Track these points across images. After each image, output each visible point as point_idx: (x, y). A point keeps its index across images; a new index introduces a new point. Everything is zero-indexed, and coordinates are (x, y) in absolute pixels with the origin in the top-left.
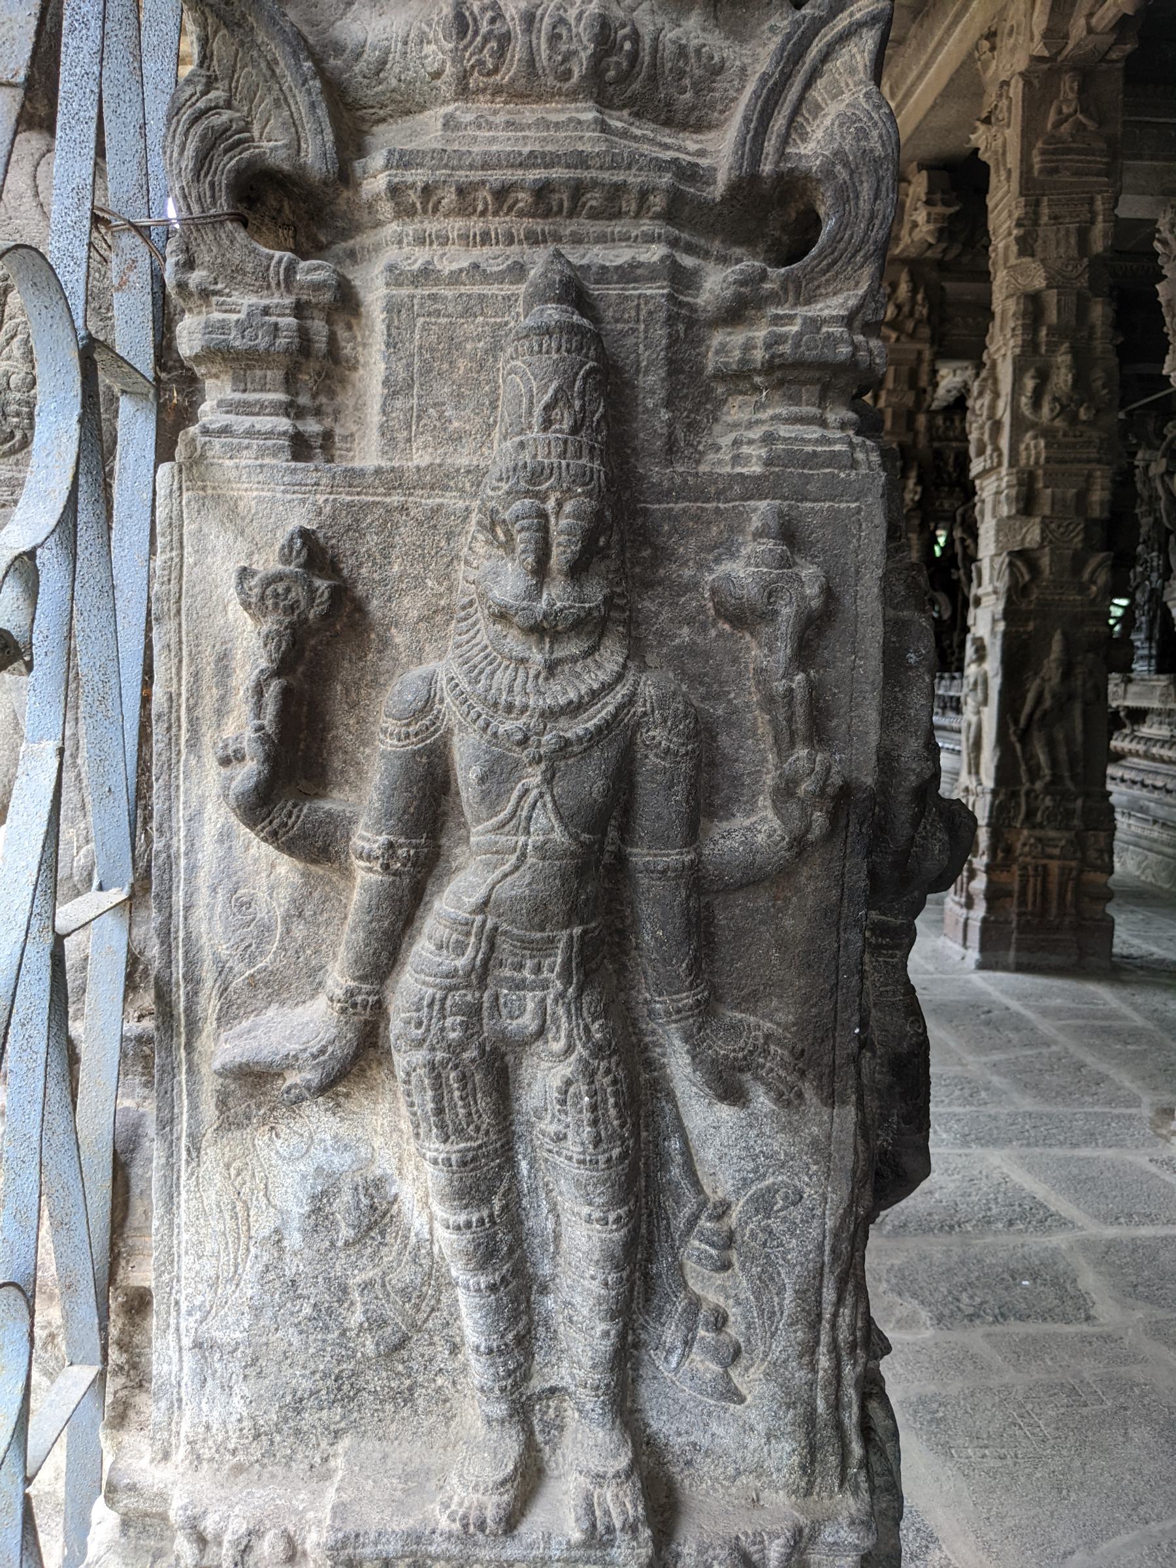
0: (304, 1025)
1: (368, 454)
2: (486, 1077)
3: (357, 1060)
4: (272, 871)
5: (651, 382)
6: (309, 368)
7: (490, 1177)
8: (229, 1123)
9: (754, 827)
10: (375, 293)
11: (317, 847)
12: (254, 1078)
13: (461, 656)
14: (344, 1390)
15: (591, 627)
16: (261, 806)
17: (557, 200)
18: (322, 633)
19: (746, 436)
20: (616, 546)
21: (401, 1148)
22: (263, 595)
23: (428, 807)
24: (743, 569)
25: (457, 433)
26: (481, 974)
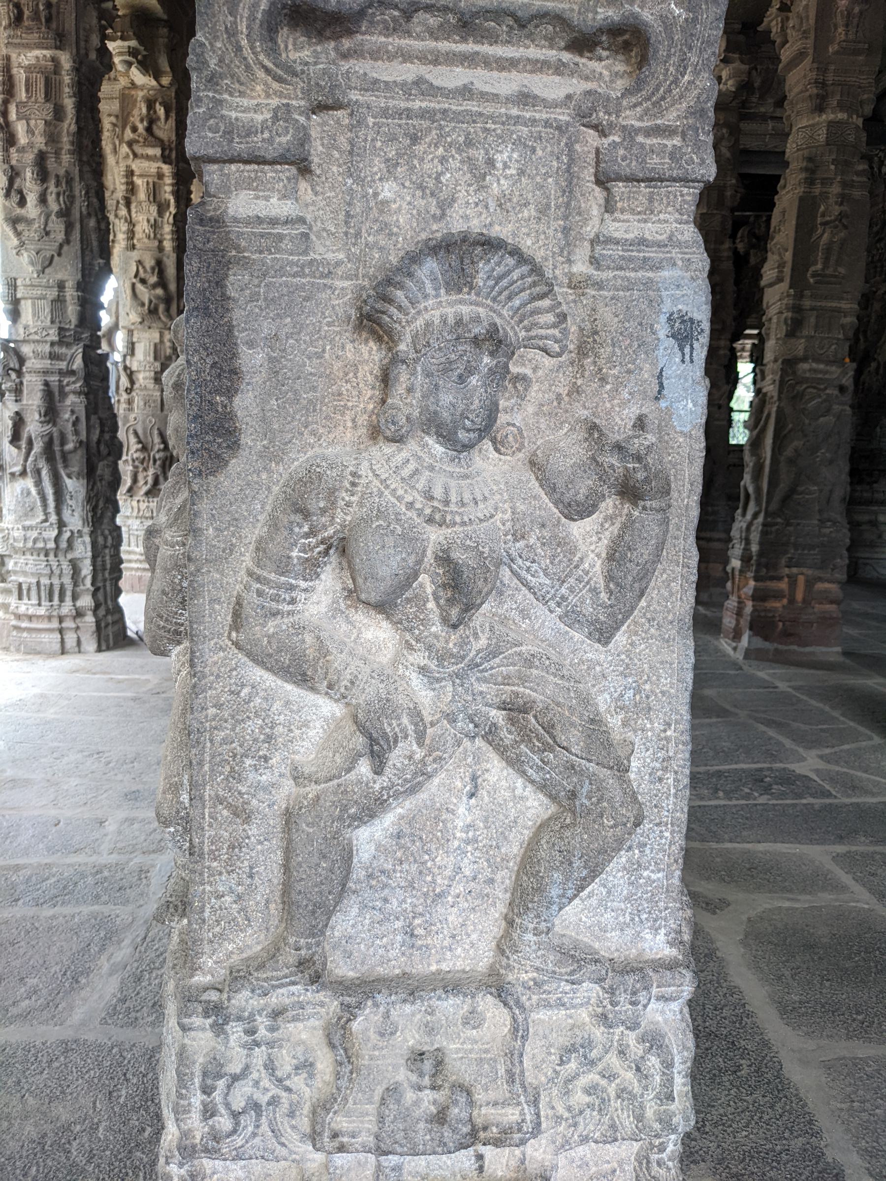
0: (17, 469)
1: (24, 402)
2: (38, 472)
3: (23, 473)
4: (15, 451)
5: (57, 394)
6: (18, 391)
7: (38, 483)
9: (70, 446)
12: (13, 475)
13: (34, 427)
14: (26, 515)
15: (48, 422)
16: (11, 442)
17: (46, 372)
18: (19, 422)
19: (71, 399)
20: (50, 413)
21: (29, 483)
22: (11, 418)
23: (30, 443)
24: (67, 416)
25: (33, 400)
26: (35, 460)
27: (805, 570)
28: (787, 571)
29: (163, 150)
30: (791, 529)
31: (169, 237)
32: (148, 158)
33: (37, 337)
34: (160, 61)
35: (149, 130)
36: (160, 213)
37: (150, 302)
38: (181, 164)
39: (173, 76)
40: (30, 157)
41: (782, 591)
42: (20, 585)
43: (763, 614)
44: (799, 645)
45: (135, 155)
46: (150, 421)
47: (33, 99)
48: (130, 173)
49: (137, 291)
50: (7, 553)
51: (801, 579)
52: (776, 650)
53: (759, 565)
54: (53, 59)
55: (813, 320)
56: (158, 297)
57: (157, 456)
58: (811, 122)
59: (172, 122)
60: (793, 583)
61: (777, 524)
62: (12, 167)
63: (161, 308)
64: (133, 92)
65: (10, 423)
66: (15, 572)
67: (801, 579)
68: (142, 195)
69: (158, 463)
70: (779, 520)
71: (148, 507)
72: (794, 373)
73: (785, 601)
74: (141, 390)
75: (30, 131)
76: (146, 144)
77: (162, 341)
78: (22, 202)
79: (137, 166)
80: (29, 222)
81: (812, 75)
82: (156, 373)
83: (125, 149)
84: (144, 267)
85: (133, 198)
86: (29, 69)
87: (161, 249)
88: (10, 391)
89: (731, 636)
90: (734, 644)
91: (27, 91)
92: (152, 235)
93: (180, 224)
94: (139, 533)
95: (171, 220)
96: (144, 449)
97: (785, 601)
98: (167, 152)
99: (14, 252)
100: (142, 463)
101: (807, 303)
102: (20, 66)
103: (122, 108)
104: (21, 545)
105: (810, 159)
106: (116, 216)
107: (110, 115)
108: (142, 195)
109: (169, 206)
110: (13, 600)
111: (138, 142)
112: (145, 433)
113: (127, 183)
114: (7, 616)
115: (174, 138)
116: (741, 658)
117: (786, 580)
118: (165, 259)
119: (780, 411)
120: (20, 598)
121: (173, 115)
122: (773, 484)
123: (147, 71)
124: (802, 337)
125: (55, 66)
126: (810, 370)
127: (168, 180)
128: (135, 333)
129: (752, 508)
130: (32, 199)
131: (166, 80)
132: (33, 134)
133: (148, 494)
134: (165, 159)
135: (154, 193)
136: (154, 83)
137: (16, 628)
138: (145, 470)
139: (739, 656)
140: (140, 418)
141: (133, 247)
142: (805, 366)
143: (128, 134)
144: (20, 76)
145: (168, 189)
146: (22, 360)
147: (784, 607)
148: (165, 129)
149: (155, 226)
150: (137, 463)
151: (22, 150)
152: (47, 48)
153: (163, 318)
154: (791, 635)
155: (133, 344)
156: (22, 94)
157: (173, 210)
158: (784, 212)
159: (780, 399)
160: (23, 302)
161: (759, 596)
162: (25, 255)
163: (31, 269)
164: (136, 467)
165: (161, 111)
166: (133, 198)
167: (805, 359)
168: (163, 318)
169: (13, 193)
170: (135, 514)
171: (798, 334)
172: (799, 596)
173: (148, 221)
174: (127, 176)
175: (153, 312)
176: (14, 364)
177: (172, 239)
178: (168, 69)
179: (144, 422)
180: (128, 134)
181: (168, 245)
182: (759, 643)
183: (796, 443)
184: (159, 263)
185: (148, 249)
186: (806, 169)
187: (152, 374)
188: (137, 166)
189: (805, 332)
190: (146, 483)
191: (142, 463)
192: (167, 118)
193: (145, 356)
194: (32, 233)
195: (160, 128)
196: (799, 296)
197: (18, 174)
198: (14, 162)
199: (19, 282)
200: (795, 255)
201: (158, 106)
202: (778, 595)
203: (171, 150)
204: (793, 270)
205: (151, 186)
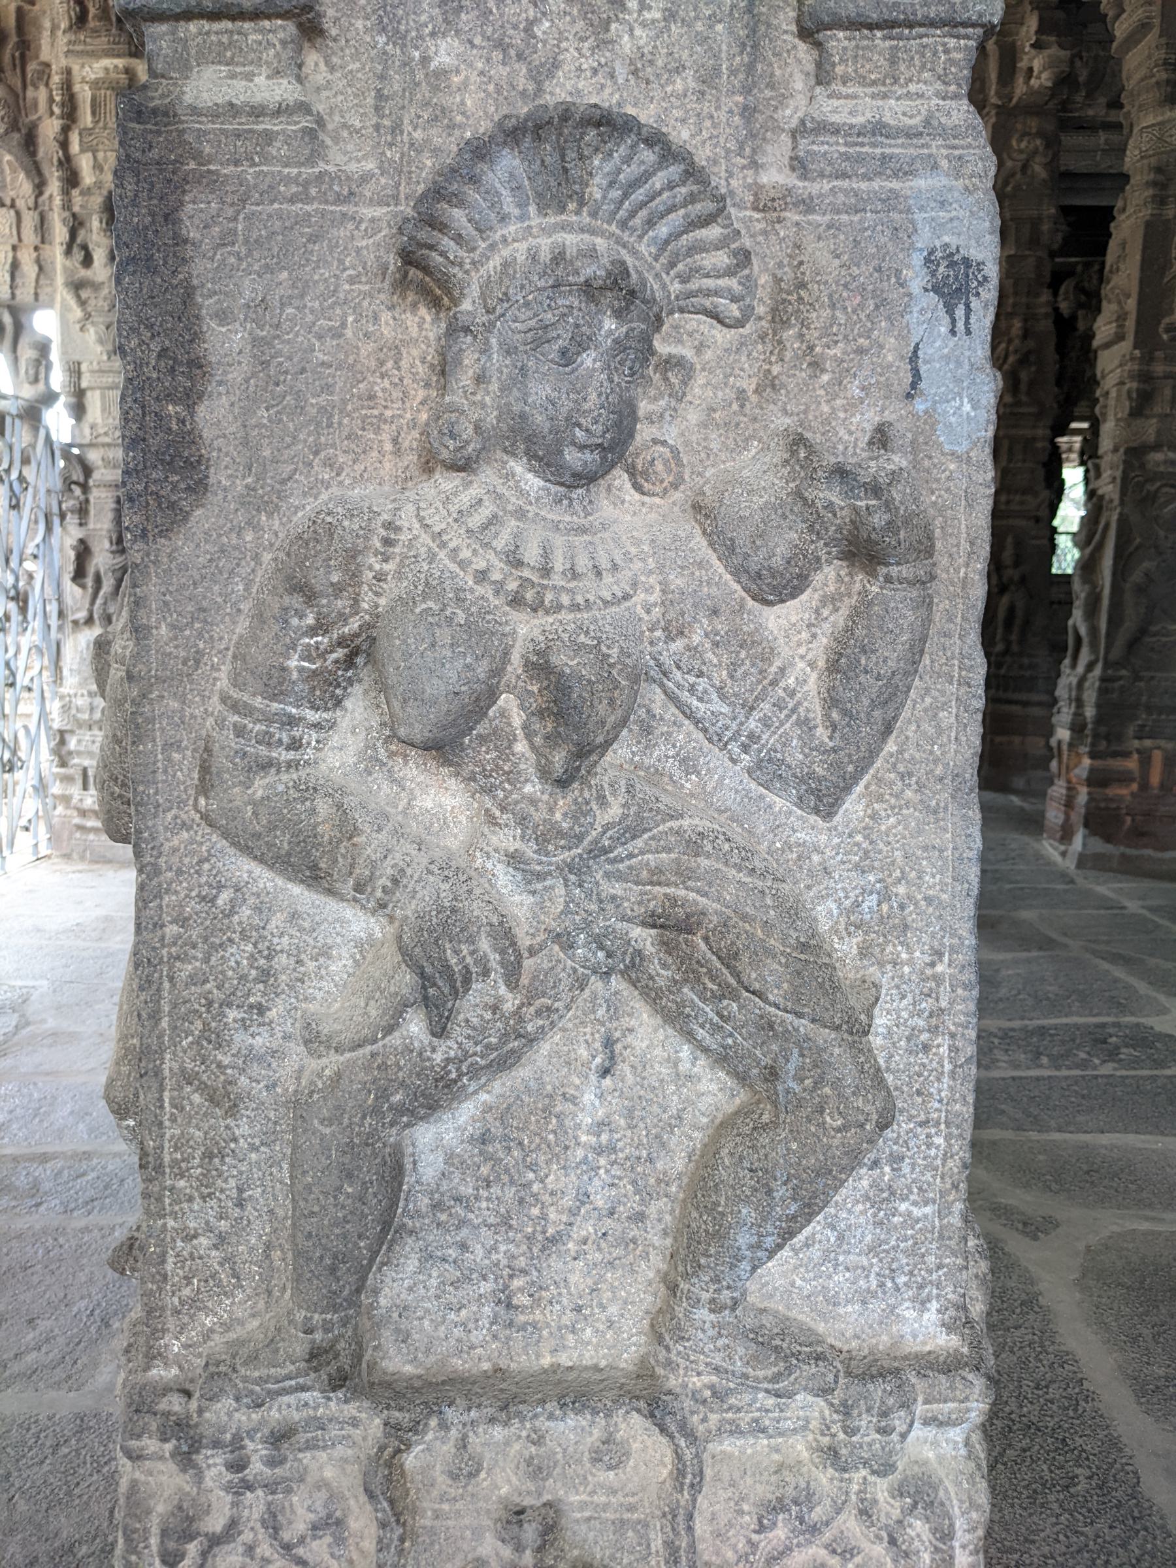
0: (82, 615)
1: (91, 526)
3: (89, 621)
4: (78, 590)
6: (82, 511)
8: (74, 632)
10: (92, 500)
11: (83, 586)
13: (102, 559)
18: (83, 552)
22: (74, 548)
23: (98, 580)
26: (105, 603)
27: (1162, 743)
28: (1136, 743)
30: (1142, 684)
33: (107, 440)
40: (97, 200)
41: (1130, 772)
42: (85, 770)
43: (1103, 805)
44: (1155, 849)
47: (101, 124)
50: (68, 728)
51: (1157, 756)
52: (1123, 855)
53: (1096, 736)
54: (127, 71)
55: (1168, 392)
58: (1160, 119)
60: (1145, 759)
61: (1120, 678)
62: (74, 215)
65: (72, 555)
66: (79, 753)
67: (1157, 756)
70: (1124, 672)
72: (1142, 466)
73: (1135, 787)
75: (97, 167)
78: (88, 261)
80: (96, 287)
81: (1161, 54)
86: (95, 85)
88: (72, 512)
89: (1058, 835)
90: (1062, 848)
91: (93, 113)
97: (1135, 787)
99: (78, 326)
101: (1159, 369)
102: (83, 81)
104: (86, 716)
105: (1159, 170)
110: (75, 791)
114: (69, 812)
116: (1073, 867)
117: (1136, 756)
119: (1123, 521)
120: (85, 788)
122: (1114, 621)
124: (1153, 416)
125: (131, 80)
126: (1165, 462)
129: (1085, 656)
130: (99, 256)
132: (101, 170)
137: (80, 828)
139: (1070, 864)
142: (1158, 456)
144: (84, 93)
146: (87, 471)
147: (1132, 794)
151: (87, 192)
152: (118, 56)
154: (1143, 834)
156: (86, 118)
158: (1123, 245)
159: (1122, 502)
160: (89, 394)
161: (1097, 780)
162: (92, 330)
163: (99, 349)
167: (1157, 447)
169: (75, 249)
171: (1147, 412)
172: (1155, 778)
176: (78, 475)
182: (1098, 846)
183: (1146, 565)
186: (1155, 184)
189: (1158, 409)
194: (99, 301)
196: (1148, 359)
197: (81, 224)
198: (76, 209)
199: (84, 367)
200: (1140, 302)
202: (1124, 778)
204: (1138, 322)
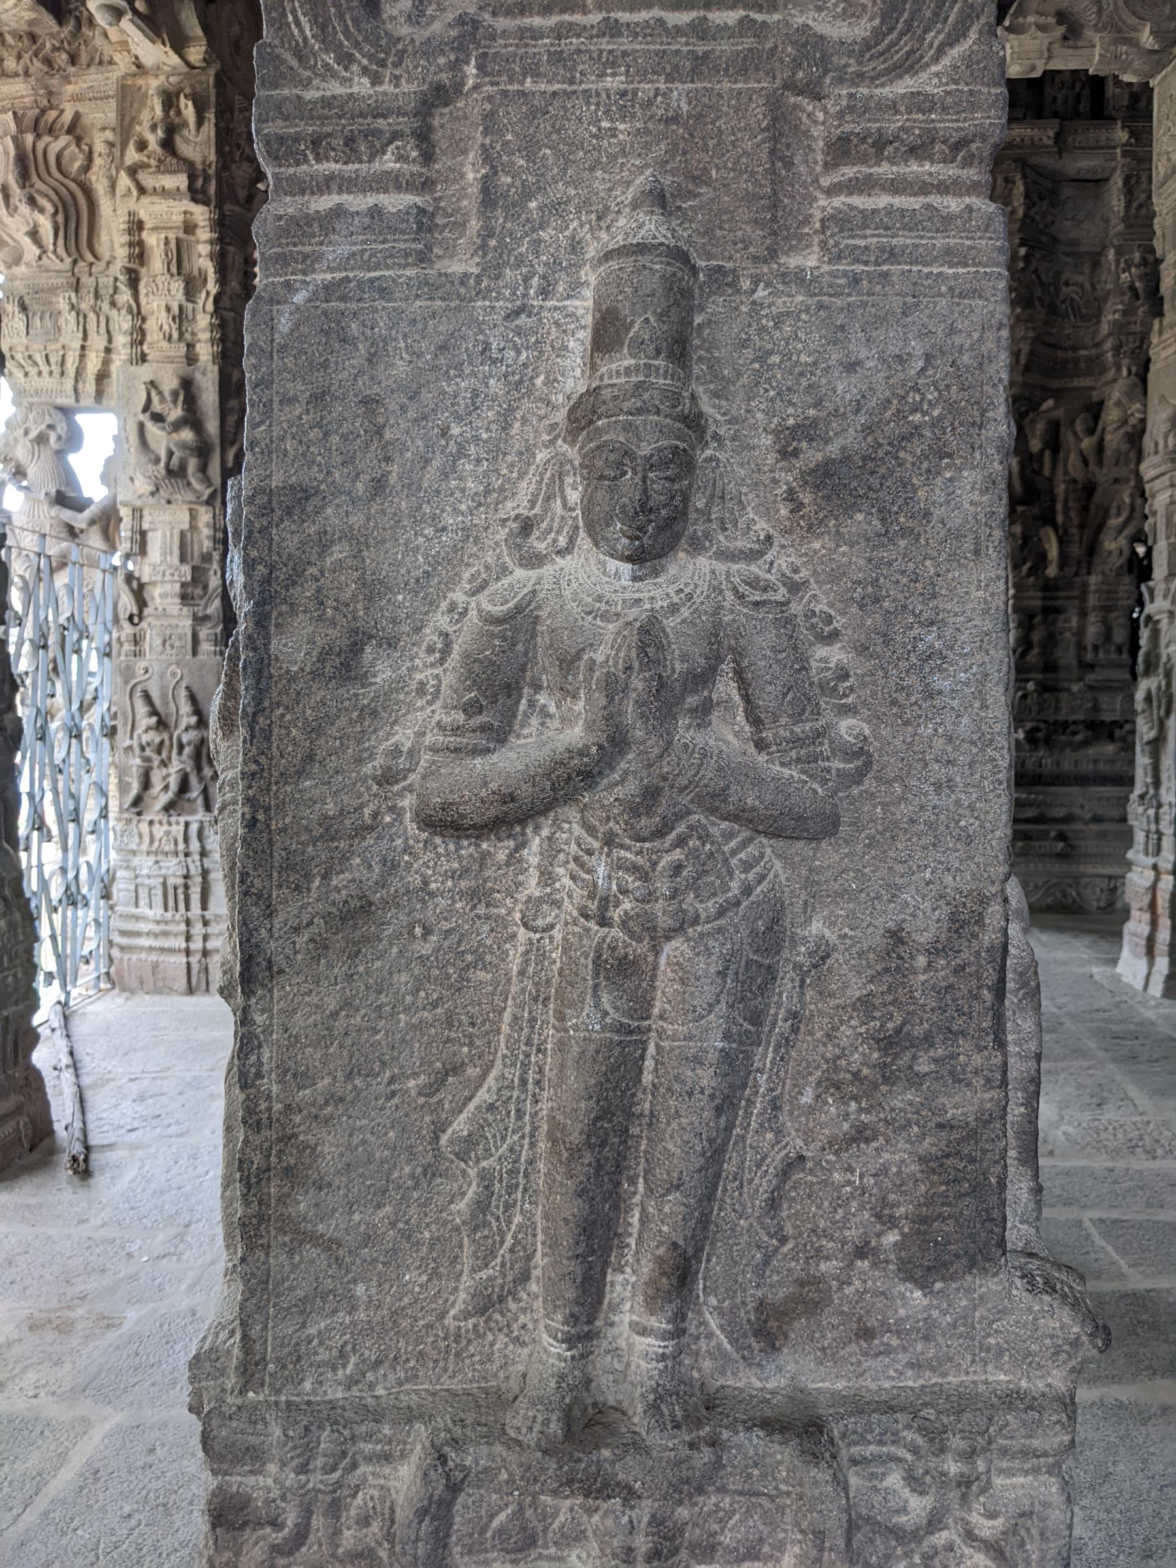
29: (192, 178)
31: (205, 336)
32: (164, 193)
34: (183, 16)
35: (168, 144)
36: (190, 293)
37: (170, 454)
38: (228, 207)
39: (209, 45)
45: (142, 190)
46: (174, 674)
48: (136, 226)
49: (149, 437)
56: (183, 446)
57: (185, 740)
59: (209, 129)
63: (192, 464)
64: (140, 82)
68: (157, 263)
69: (187, 750)
71: (168, 833)
74: (157, 617)
76: (162, 168)
77: (193, 527)
79: (148, 209)
82: (183, 585)
83: (124, 181)
84: (160, 393)
85: (143, 271)
87: (191, 359)
92: (175, 335)
93: (229, 315)
94: (152, 881)
95: (210, 306)
96: (162, 724)
98: (199, 183)
100: (159, 752)
103: (122, 113)
106: (113, 304)
107: (104, 129)
108: (157, 263)
109: (205, 280)
111: (147, 166)
112: (164, 696)
113: (131, 244)
115: (213, 157)
118: (198, 376)
121: (211, 116)
123: (158, 35)
127: (204, 234)
128: (146, 512)
131: (196, 53)
133: (168, 808)
134: (196, 194)
135: (179, 257)
136: (175, 60)
138: (164, 764)
140: (156, 669)
141: (143, 358)
143: (132, 156)
145: (204, 249)
148: (198, 143)
149: (181, 318)
150: (148, 752)
153: (196, 485)
155: (143, 534)
157: (212, 287)
164: (147, 760)
165: (188, 110)
166: (143, 271)
168: (196, 485)
170: (145, 846)
173: (168, 309)
174: (130, 232)
175: (176, 473)
177: (212, 340)
178: (200, 33)
179: (162, 676)
180: (132, 156)
181: (205, 351)
184: (187, 384)
185: (169, 360)
187: (177, 587)
188: (148, 209)
190: (166, 788)
191: (159, 751)
192: (200, 121)
193: (164, 554)
195: (187, 141)
201: (182, 100)
203: (207, 179)
205: (173, 246)
